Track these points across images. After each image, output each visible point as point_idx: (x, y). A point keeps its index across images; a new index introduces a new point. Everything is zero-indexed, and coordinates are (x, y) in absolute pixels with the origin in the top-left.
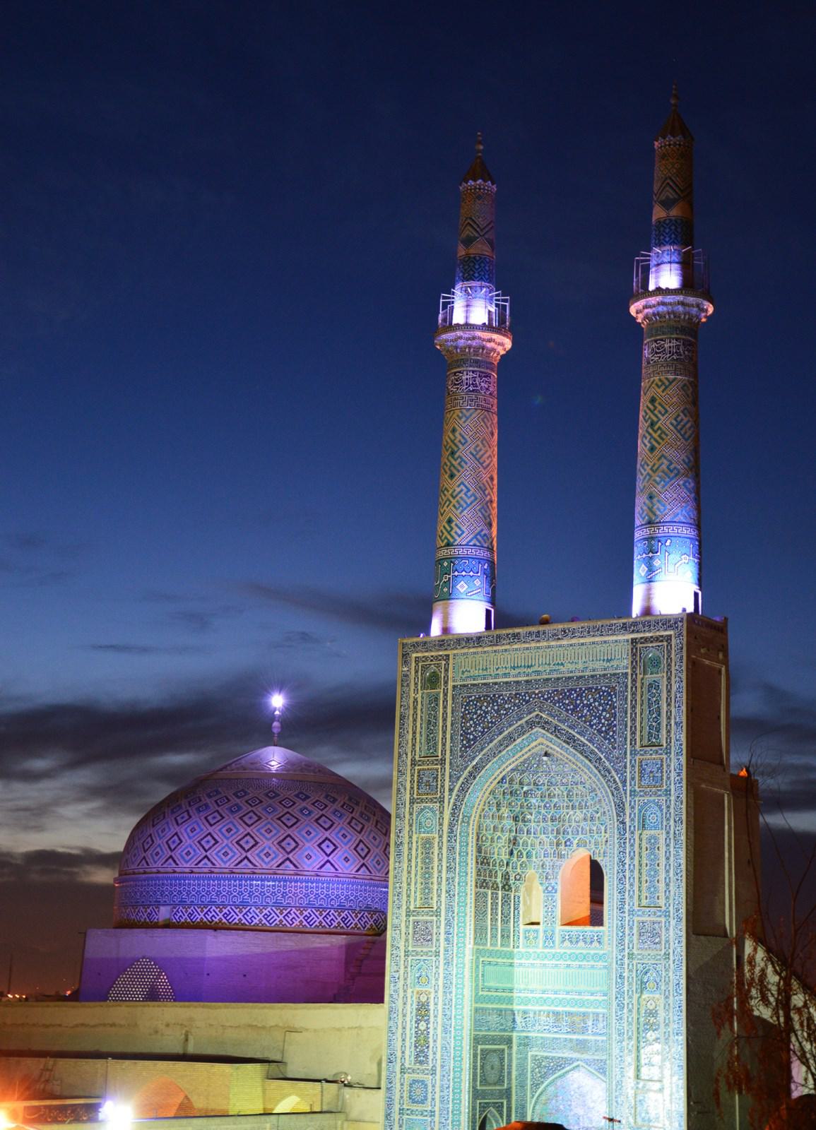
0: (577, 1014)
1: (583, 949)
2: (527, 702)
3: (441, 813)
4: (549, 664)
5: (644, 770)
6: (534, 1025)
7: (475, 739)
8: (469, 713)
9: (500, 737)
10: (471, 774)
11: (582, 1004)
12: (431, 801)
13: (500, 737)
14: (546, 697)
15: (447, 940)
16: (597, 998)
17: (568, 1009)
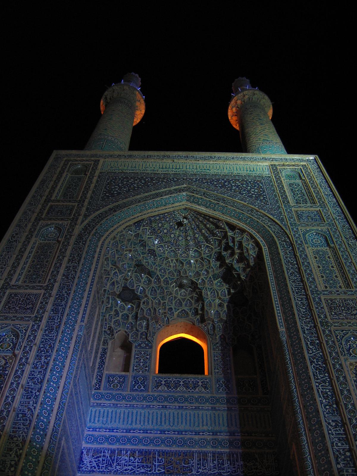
0: (176, 453)
1: (184, 392)
2: (175, 181)
3: (72, 227)
4: (196, 169)
5: (301, 215)
6: (111, 466)
7: (119, 194)
8: (114, 183)
9: (146, 194)
10: (110, 209)
11: (183, 443)
12: (62, 219)
13: (146, 194)
14: (194, 180)
15: (55, 310)
16: (203, 437)
17: (163, 448)
